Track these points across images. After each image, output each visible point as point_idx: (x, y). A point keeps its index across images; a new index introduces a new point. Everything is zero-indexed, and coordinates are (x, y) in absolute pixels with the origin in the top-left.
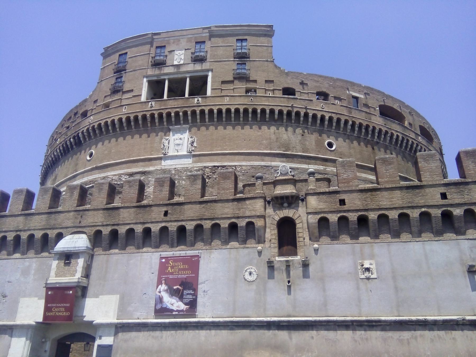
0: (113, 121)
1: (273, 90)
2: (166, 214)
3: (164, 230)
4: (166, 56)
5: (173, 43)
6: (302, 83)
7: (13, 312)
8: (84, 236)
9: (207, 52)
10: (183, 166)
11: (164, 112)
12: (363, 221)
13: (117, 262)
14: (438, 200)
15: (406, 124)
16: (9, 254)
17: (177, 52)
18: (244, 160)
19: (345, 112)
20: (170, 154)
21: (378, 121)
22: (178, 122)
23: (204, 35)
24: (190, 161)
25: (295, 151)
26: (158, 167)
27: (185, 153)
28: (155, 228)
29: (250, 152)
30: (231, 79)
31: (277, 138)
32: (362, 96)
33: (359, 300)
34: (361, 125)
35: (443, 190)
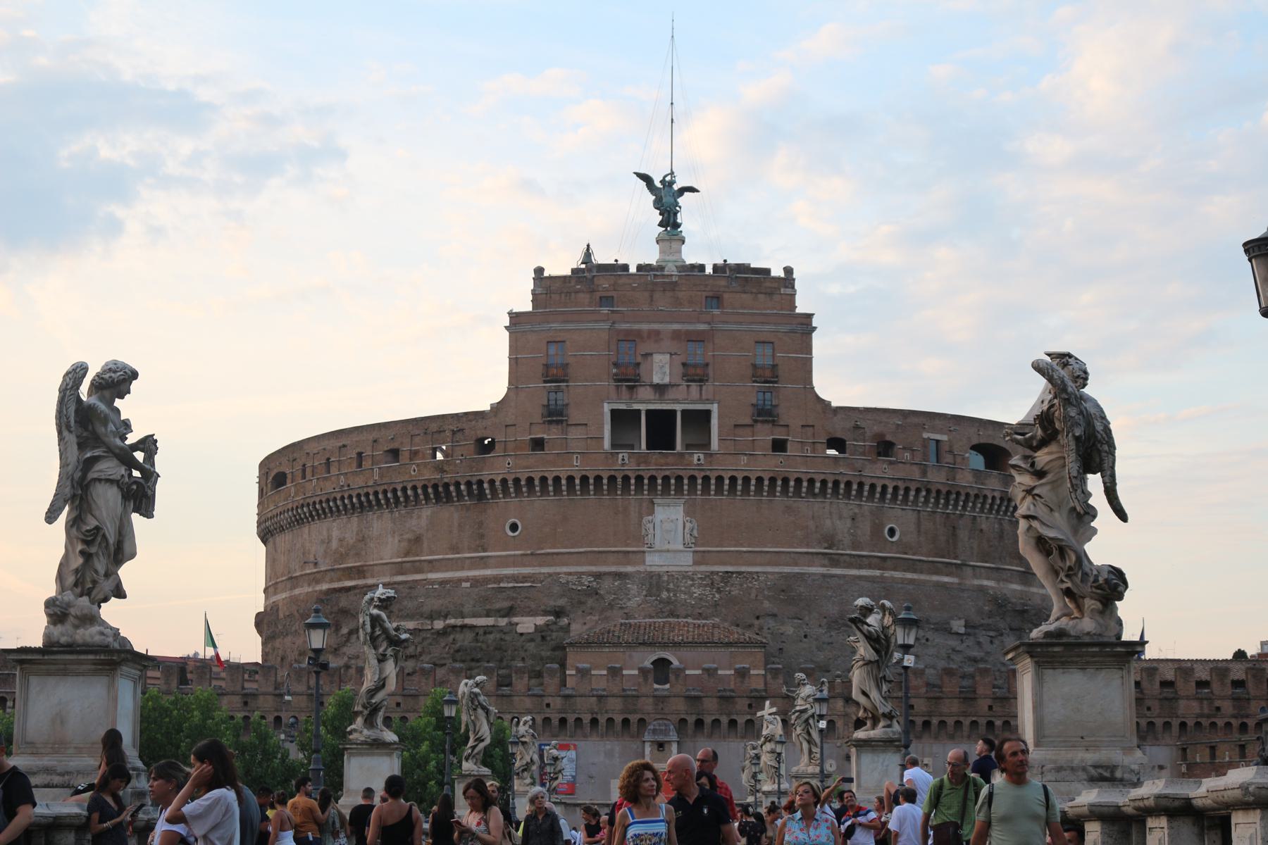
0: (557, 480)
2: (750, 706)
4: (638, 364)
6: (857, 427)
9: (707, 365)
11: (646, 475)
12: (927, 724)
16: (585, 736)
17: (657, 358)
19: (916, 474)
23: (702, 327)
26: (641, 568)
28: (741, 720)
29: (777, 548)
30: (748, 421)
32: (944, 438)
34: (938, 492)
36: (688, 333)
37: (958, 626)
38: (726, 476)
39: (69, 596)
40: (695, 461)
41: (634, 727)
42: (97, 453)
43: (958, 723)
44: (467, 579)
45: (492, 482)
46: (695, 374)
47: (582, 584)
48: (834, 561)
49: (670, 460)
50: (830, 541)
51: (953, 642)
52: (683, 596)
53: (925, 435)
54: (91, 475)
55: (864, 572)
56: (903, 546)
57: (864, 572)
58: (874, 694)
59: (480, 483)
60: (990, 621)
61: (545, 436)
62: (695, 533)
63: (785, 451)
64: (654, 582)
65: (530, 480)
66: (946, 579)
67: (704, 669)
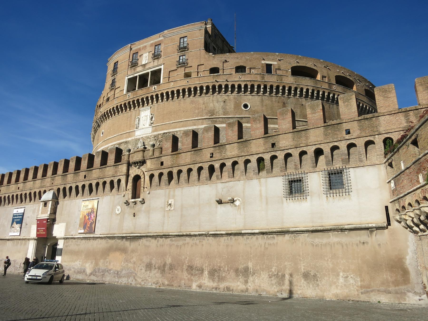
5: (143, 49)
15: (319, 77)
17: (144, 55)
19: (259, 78)
21: (290, 80)
25: (218, 115)
26: (133, 138)
30: (175, 68)
32: (275, 63)
33: (164, 224)
35: (211, 150)
36: (156, 42)
38: (164, 92)
40: (153, 89)
43: (190, 170)
46: (156, 56)
50: (212, 112)
53: (263, 62)
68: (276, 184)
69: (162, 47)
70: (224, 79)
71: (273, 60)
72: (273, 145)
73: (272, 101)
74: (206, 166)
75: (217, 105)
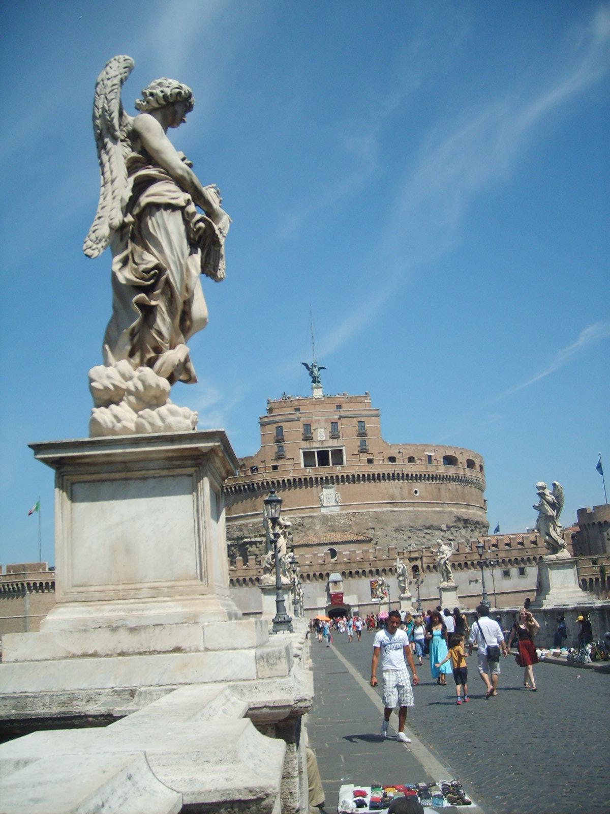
1: (383, 459)
2: (370, 564)
3: (371, 572)
5: (316, 422)
7: (316, 603)
8: (338, 574)
10: (335, 513)
13: (354, 582)
14: (463, 558)
17: (319, 430)
18: (370, 508)
20: (325, 505)
22: (327, 483)
24: (338, 508)
26: (319, 514)
27: (335, 504)
28: (367, 570)
30: (357, 453)
31: (387, 492)
34: (432, 475)
35: (465, 555)
36: (331, 419)
37: (444, 527)
39: (125, 365)
41: (324, 577)
42: (151, 171)
44: (250, 523)
45: (257, 484)
46: (334, 436)
47: (296, 521)
48: (394, 504)
49: (327, 469)
50: (393, 497)
51: (443, 534)
52: (337, 524)
53: (425, 453)
54: (144, 200)
55: (407, 509)
56: (421, 497)
57: (407, 509)
58: (553, 534)
59: (253, 484)
60: (455, 524)
61: (278, 464)
62: (340, 498)
63: (373, 463)
64: (325, 519)
65: (273, 482)
66: (438, 509)
67: (350, 551)
68: (498, 572)
69: (340, 427)
70: (400, 469)
71: (432, 452)
72: (497, 555)
73: (432, 488)
74: (463, 563)
75: (395, 490)
